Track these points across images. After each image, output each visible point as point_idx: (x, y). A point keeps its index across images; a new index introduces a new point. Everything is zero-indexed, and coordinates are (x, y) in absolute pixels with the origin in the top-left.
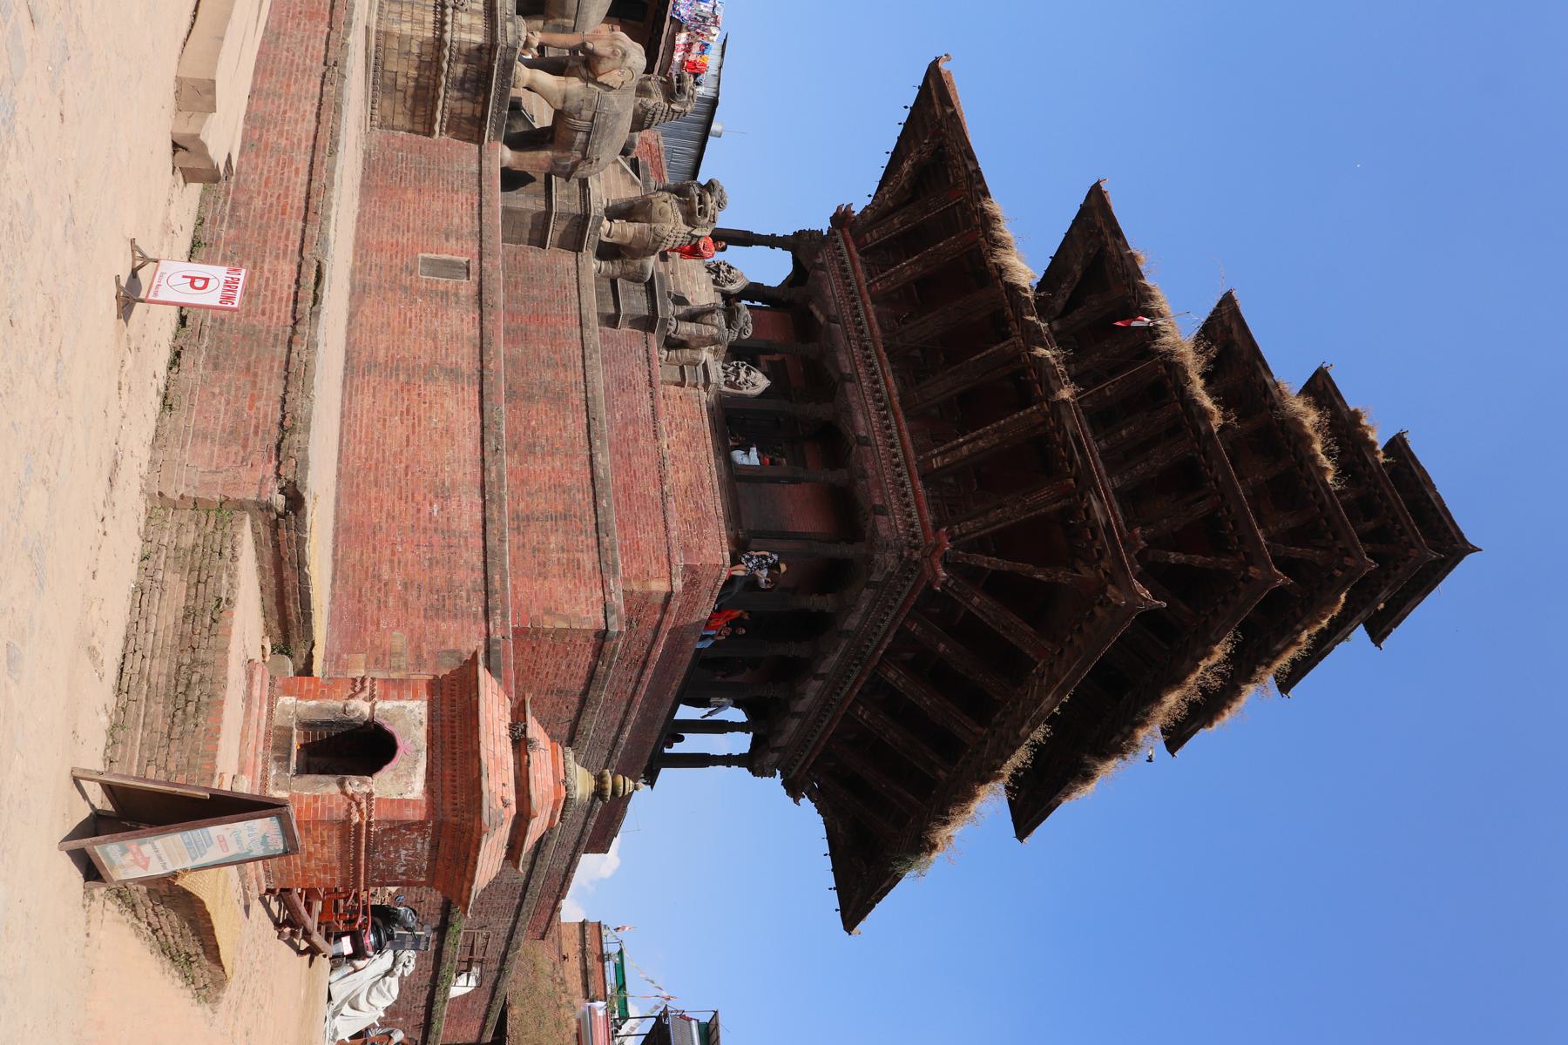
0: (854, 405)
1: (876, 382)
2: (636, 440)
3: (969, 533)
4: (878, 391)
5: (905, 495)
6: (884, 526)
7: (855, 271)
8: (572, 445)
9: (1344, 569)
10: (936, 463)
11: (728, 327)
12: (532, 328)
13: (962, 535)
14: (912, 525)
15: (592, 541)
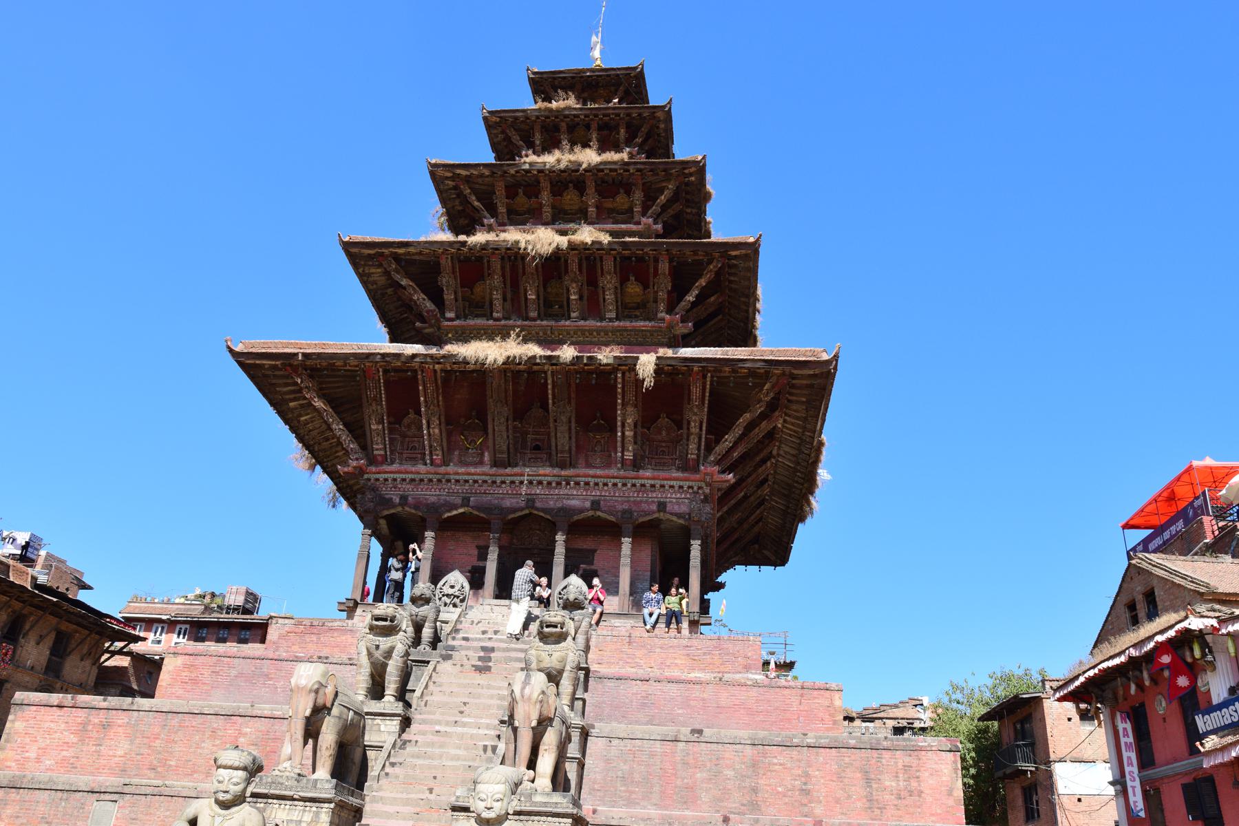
0: (559, 505)
1: (540, 483)
2: (704, 699)
3: (699, 449)
4: (549, 483)
5: (653, 486)
6: (676, 507)
7: (418, 473)
8: (799, 761)
9: (691, 174)
10: (629, 456)
11: (583, 608)
12: (679, 782)
13: (698, 456)
14: (681, 487)
15: (886, 755)
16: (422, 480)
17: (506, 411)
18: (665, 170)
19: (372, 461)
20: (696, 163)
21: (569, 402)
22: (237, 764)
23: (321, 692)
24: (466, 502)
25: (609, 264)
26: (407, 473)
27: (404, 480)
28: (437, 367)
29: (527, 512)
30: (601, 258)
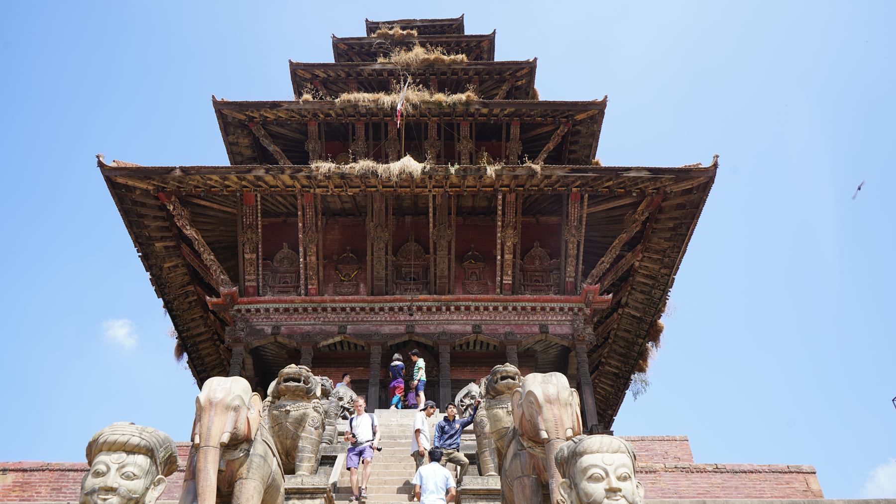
0: (440, 329)
1: (420, 309)
3: (576, 271)
4: (429, 309)
5: (534, 309)
7: (292, 302)
10: (508, 280)
13: (576, 278)
14: (561, 309)
16: (296, 310)
17: (386, 236)
18: (499, 74)
19: (243, 292)
20: (528, 62)
21: (450, 226)
22: (135, 440)
23: (243, 413)
24: (342, 331)
25: (465, 130)
26: (280, 302)
27: (277, 310)
28: (318, 190)
29: (406, 338)
30: (459, 125)
